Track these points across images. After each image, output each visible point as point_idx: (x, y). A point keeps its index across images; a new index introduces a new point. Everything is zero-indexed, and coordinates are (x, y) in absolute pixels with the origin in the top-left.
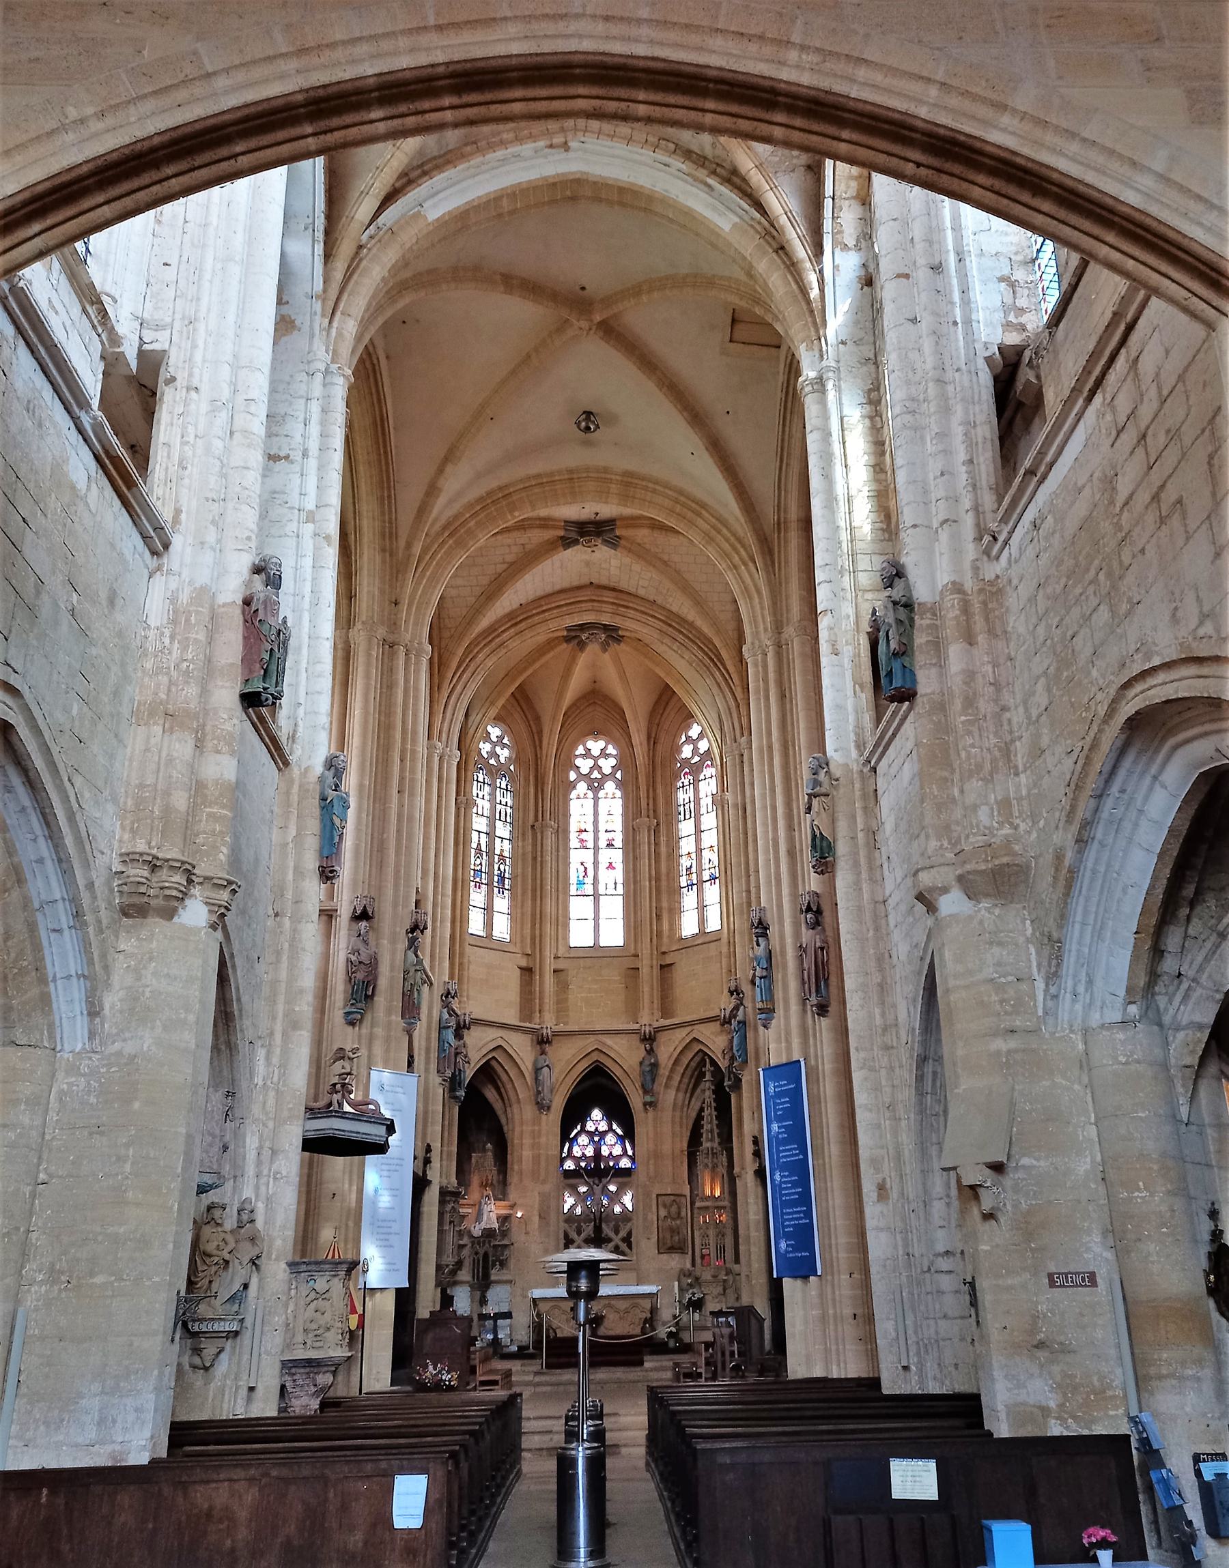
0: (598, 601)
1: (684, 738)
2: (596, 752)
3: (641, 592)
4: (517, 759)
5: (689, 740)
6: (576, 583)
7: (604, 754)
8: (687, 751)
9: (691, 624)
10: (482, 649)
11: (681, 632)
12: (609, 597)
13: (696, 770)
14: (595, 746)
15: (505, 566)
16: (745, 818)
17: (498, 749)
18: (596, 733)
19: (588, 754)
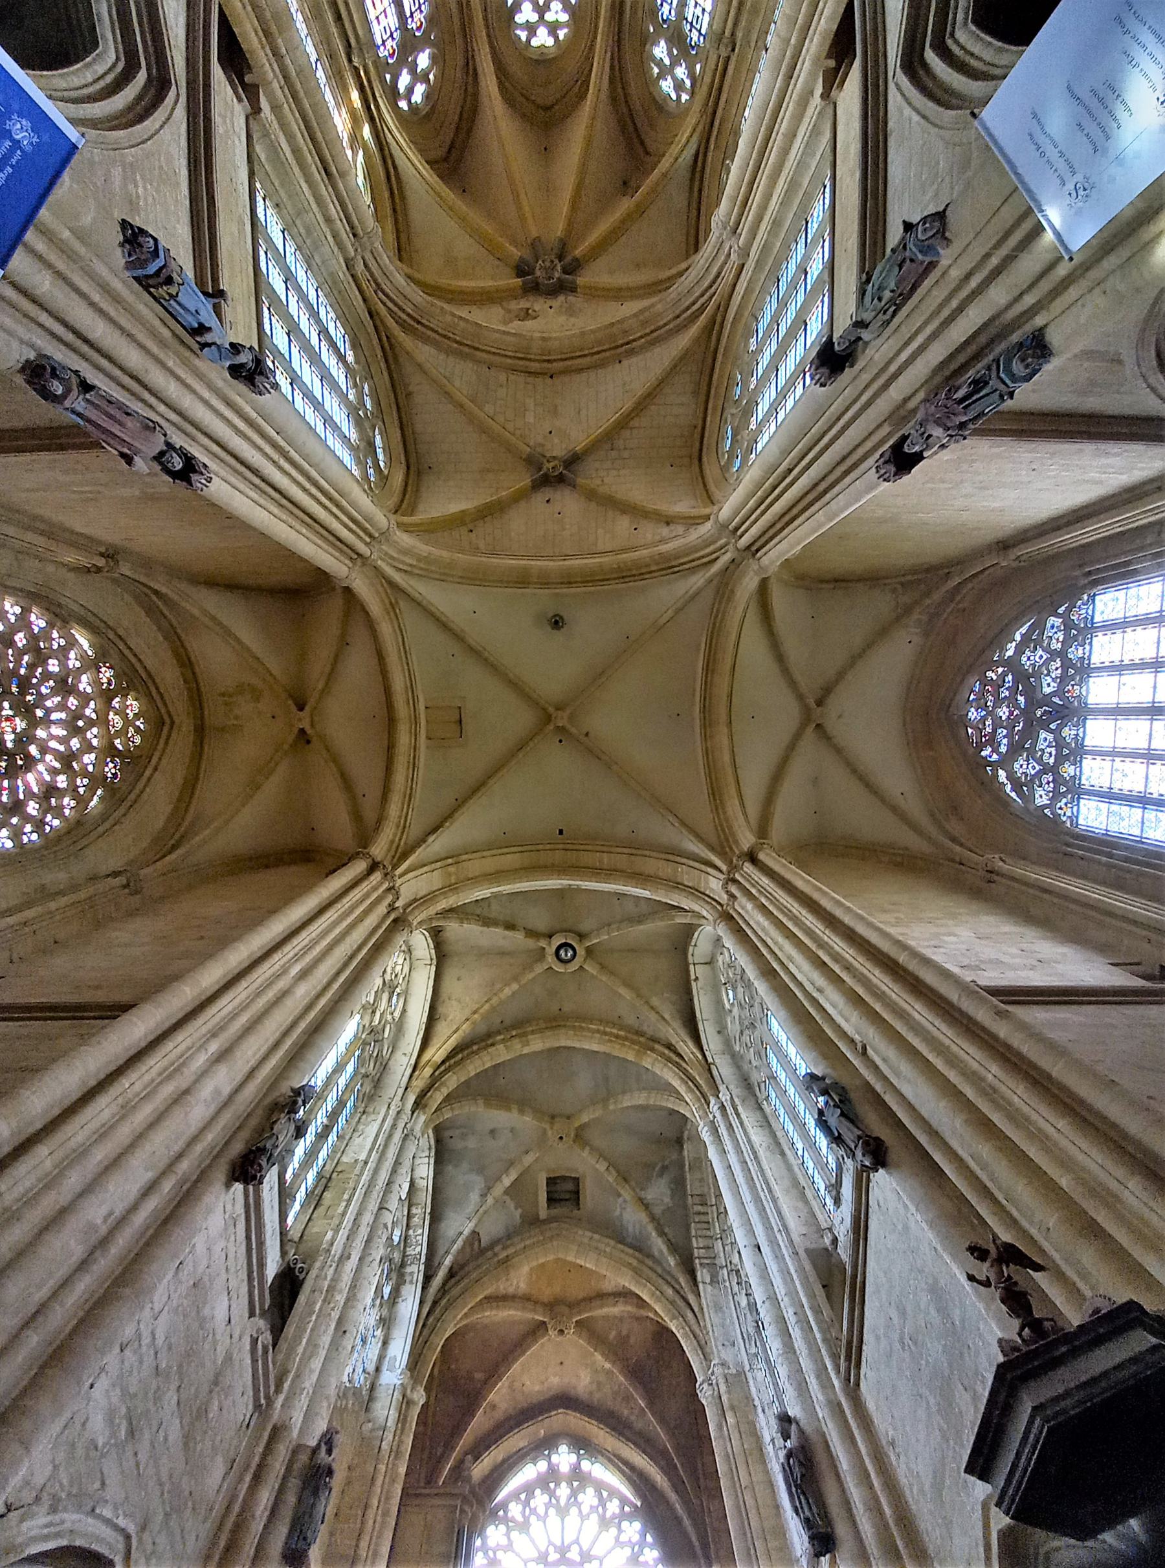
0: (545, 361)
1: (431, 77)
2: (542, 32)
3: (502, 377)
4: (645, 41)
5: (424, 78)
6: (566, 379)
7: (531, 29)
8: (423, 60)
9: (448, 352)
10: (665, 325)
11: (457, 342)
12: (535, 366)
13: (408, 45)
14: (543, 38)
15: (632, 424)
16: (322, 160)
17: (667, 61)
18: (542, 61)
19: (553, 28)
